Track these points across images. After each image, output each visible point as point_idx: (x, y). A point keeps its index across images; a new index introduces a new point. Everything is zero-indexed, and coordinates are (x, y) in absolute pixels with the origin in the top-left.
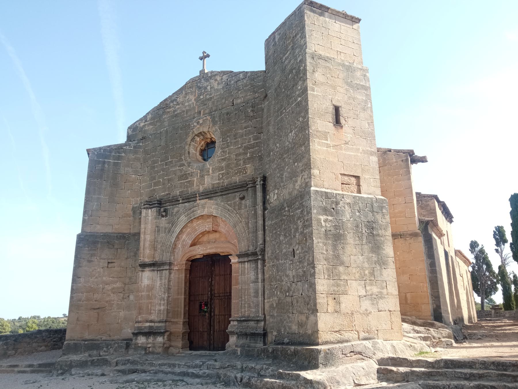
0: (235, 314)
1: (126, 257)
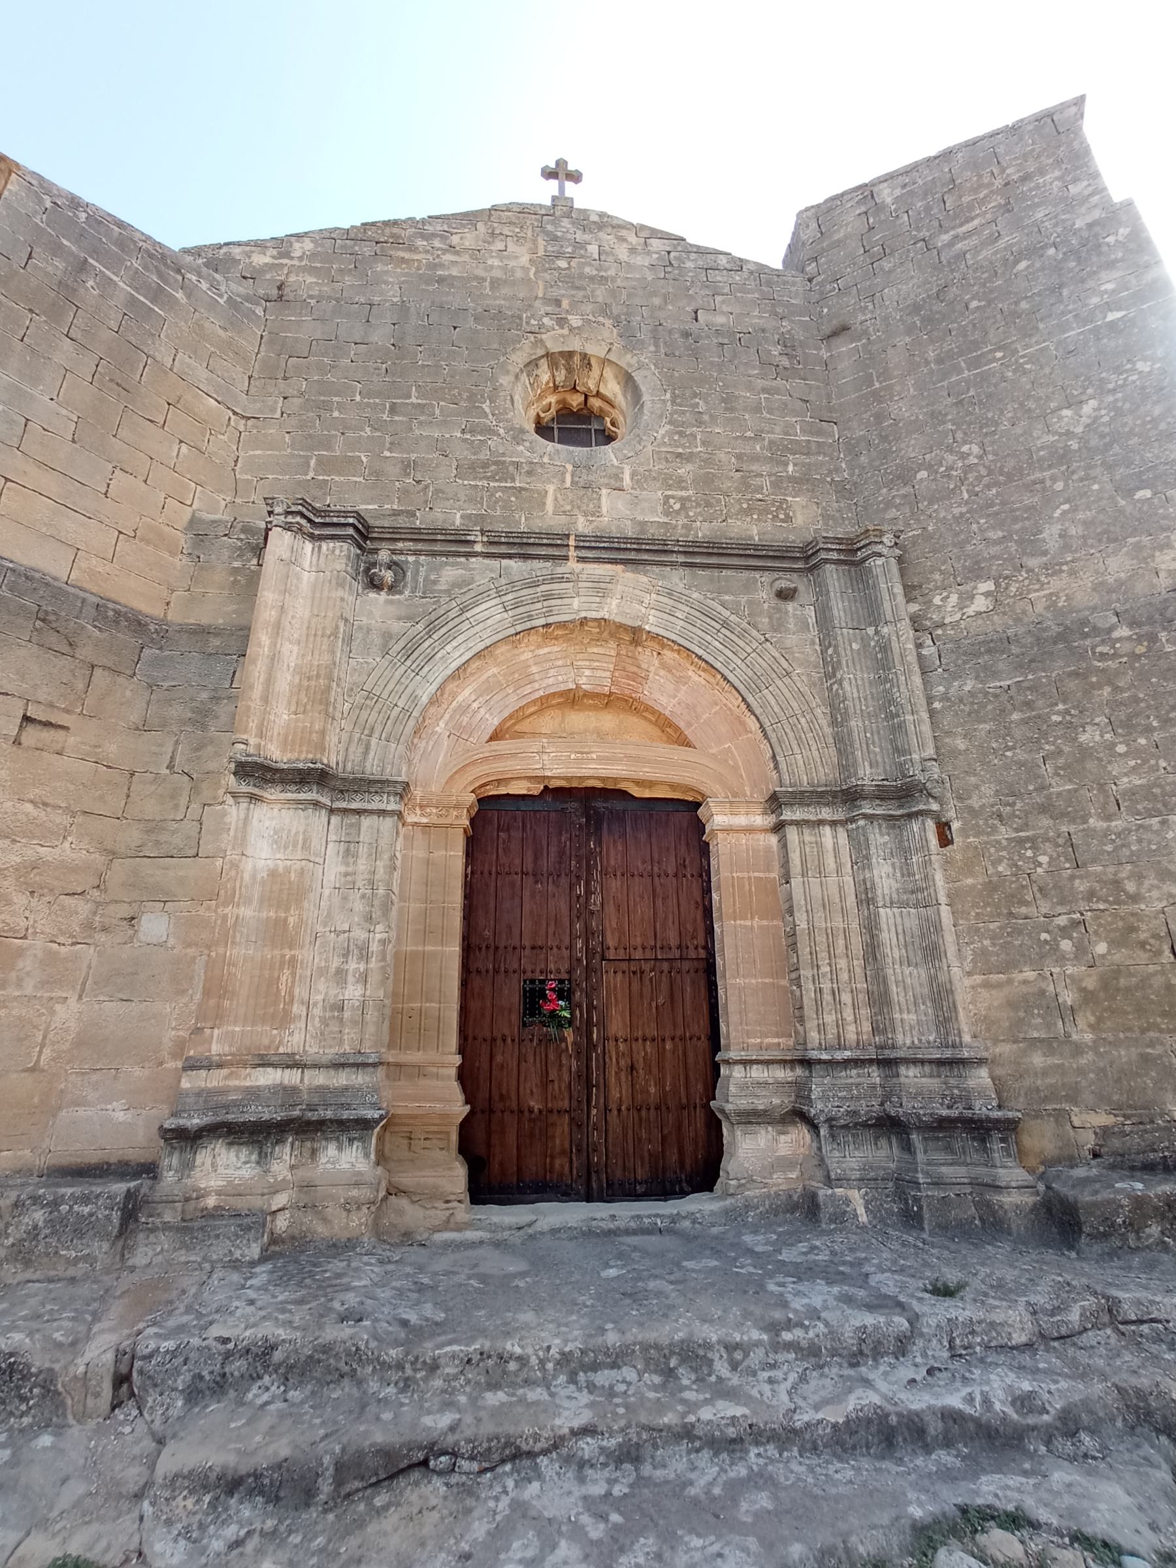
1: (134, 717)
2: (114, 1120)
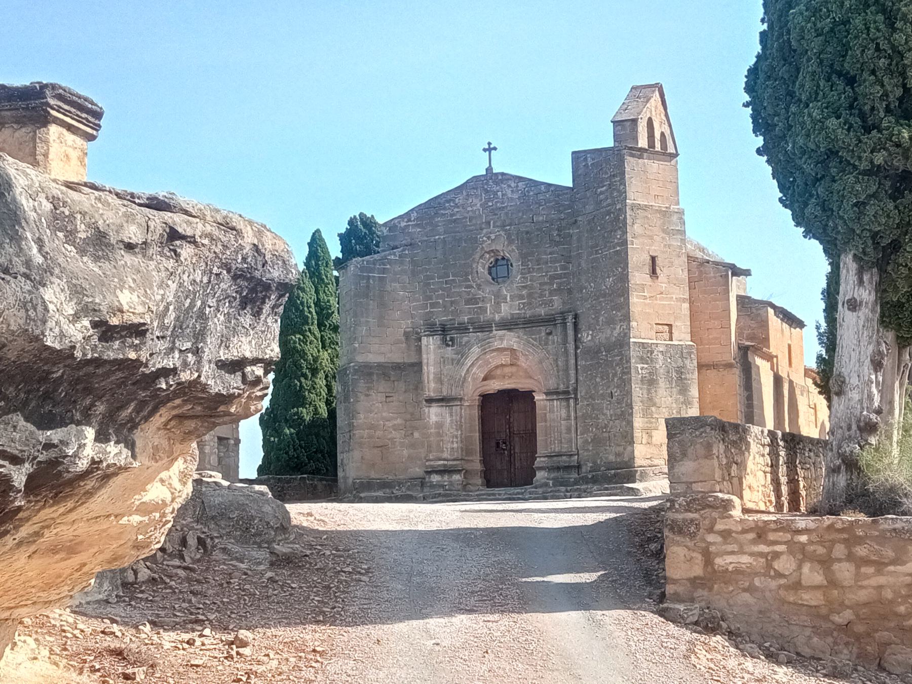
0: (541, 450)
1: (403, 389)
2: (418, 471)
